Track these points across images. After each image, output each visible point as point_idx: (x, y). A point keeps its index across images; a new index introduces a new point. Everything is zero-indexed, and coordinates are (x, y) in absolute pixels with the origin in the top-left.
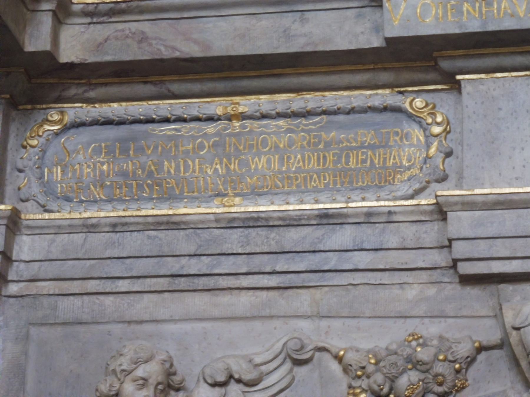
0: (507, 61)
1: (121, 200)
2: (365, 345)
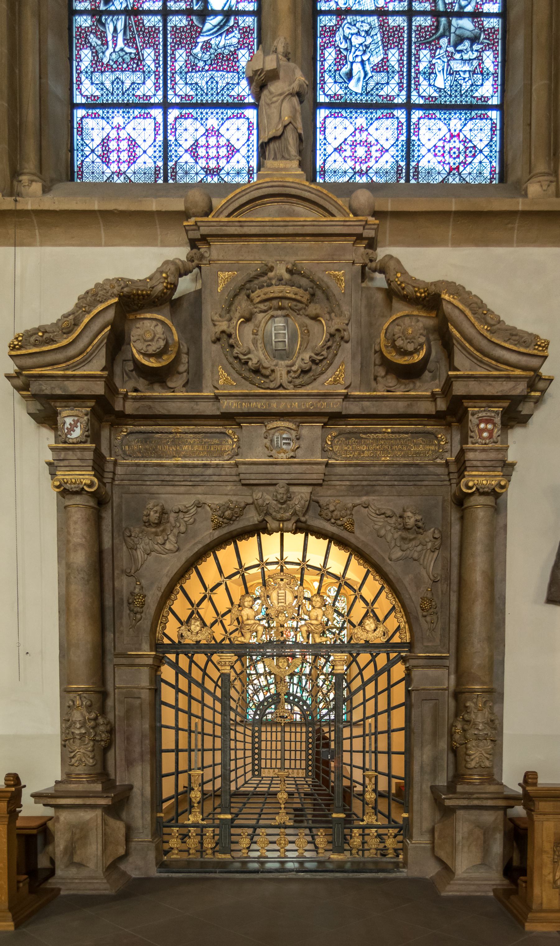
0: (255, 420)
1: (146, 457)
2: (217, 503)
